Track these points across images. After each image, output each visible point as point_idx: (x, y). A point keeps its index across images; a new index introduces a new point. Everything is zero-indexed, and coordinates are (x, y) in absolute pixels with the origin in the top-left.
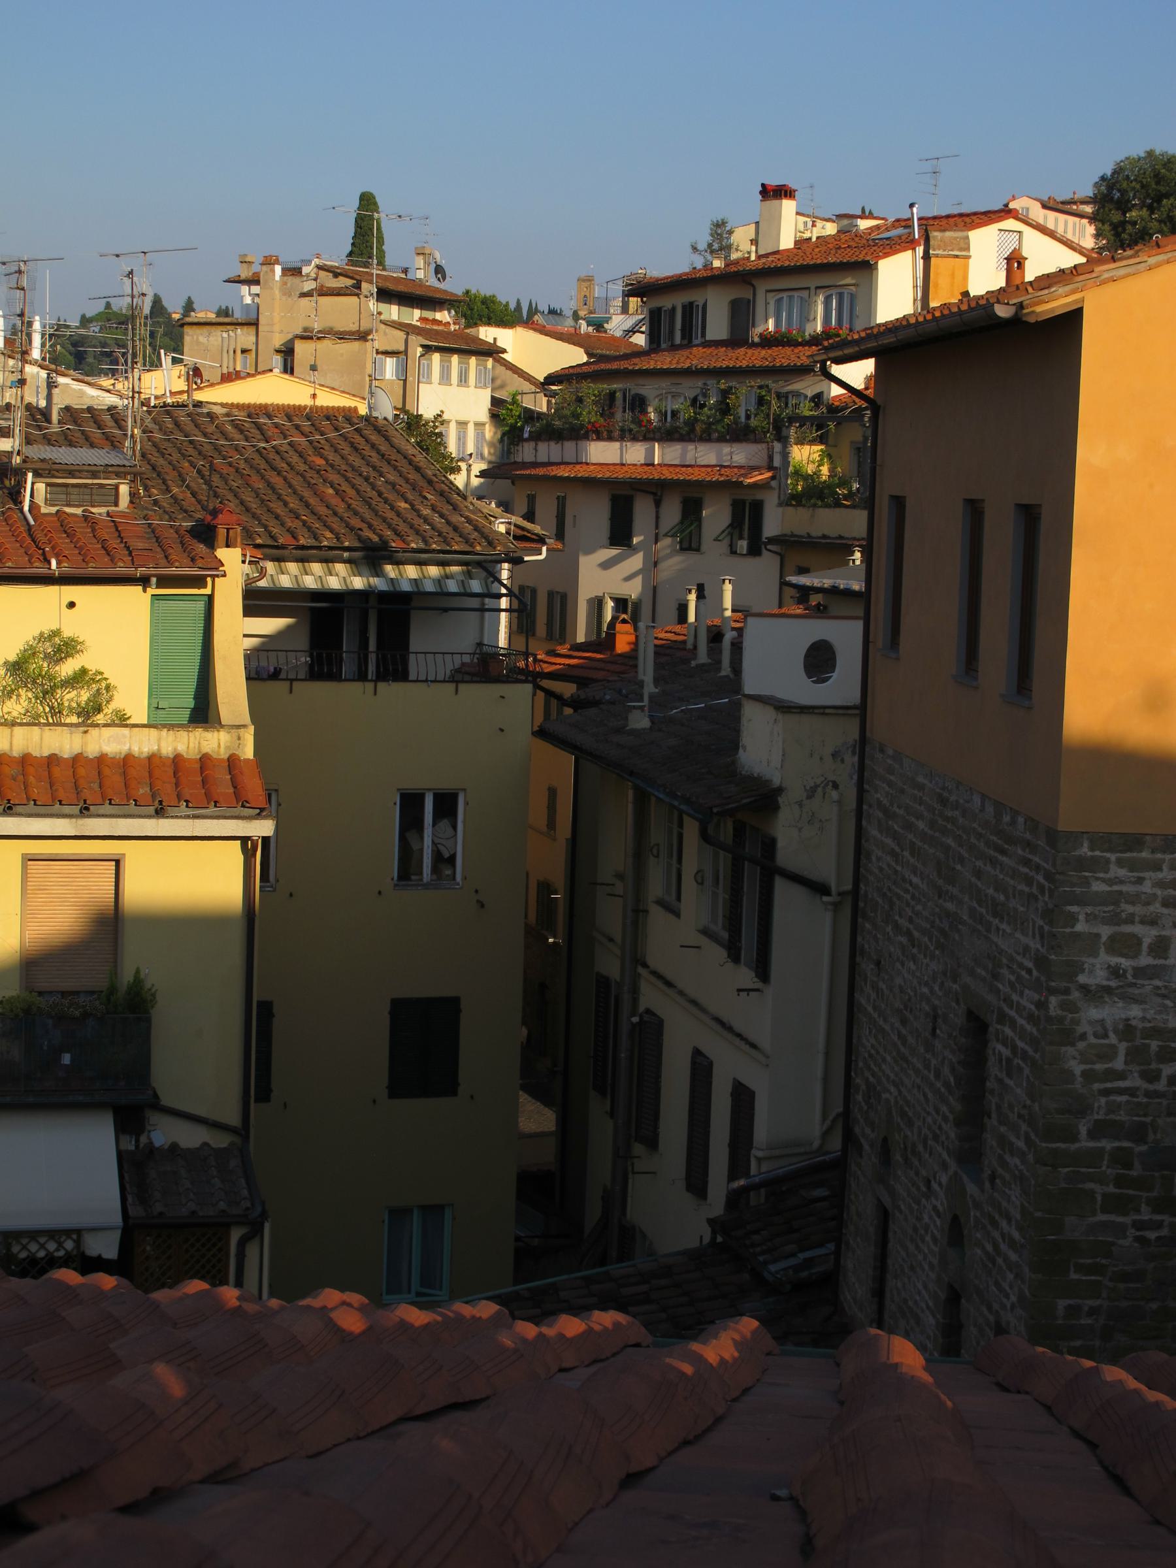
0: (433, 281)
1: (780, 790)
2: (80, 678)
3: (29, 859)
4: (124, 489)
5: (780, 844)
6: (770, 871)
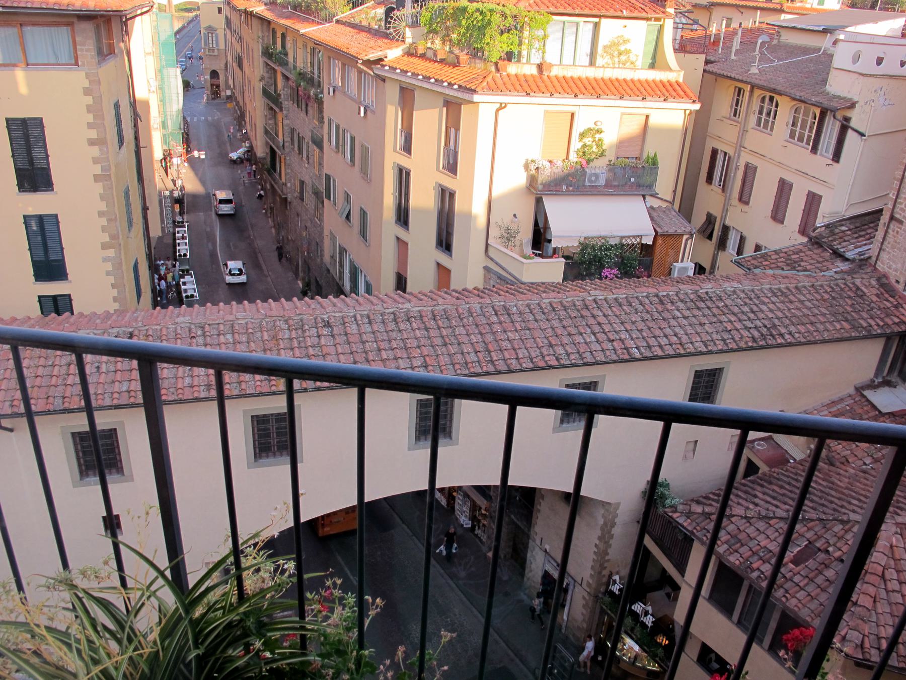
1: (857, 102)
2: (627, 52)
3: (623, 114)
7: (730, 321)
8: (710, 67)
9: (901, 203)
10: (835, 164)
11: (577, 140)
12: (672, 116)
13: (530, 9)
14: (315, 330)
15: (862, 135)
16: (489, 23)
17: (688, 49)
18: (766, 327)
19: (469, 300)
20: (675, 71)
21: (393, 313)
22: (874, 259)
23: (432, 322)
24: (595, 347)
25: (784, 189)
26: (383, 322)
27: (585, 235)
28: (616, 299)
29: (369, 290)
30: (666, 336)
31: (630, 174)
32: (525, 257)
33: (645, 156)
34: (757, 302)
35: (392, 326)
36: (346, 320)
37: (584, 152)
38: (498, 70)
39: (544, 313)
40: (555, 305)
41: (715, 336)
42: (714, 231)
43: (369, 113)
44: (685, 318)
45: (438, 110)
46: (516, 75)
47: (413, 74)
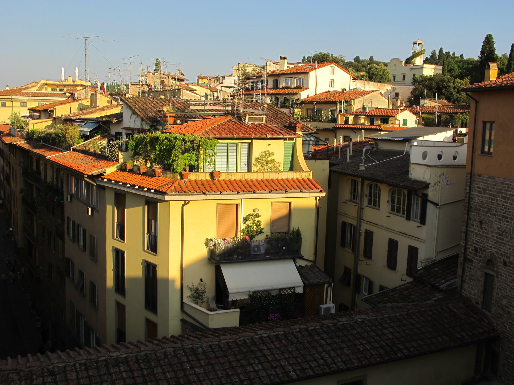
0: (181, 76)
1: (429, 184)
2: (273, 161)
3: (272, 203)
4: (264, 118)
5: (429, 195)
6: (425, 200)
7: (362, 344)
8: (334, 168)
9: (469, 248)
10: (423, 226)
11: (242, 223)
12: (308, 200)
13: (202, 136)
14: (41, 379)
15: (436, 205)
16: (174, 146)
17: (317, 157)
18: (388, 345)
19: (165, 345)
20: (306, 172)
21: (105, 360)
22: (459, 288)
23: (136, 365)
24: (262, 373)
25: (393, 245)
26: (97, 368)
27: (253, 290)
28: (277, 336)
29: (98, 343)
30: (315, 360)
31: (281, 243)
32: (210, 310)
33: (292, 229)
34: (381, 328)
35: (103, 371)
36: (68, 369)
37: (248, 231)
38: (182, 178)
39: (222, 351)
40: (231, 344)
41: (351, 356)
42: (352, 280)
43: (95, 212)
44: (329, 345)
45: (141, 208)
46: (195, 181)
47: (123, 183)
